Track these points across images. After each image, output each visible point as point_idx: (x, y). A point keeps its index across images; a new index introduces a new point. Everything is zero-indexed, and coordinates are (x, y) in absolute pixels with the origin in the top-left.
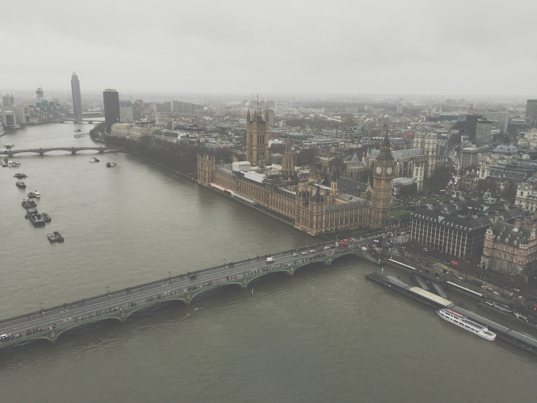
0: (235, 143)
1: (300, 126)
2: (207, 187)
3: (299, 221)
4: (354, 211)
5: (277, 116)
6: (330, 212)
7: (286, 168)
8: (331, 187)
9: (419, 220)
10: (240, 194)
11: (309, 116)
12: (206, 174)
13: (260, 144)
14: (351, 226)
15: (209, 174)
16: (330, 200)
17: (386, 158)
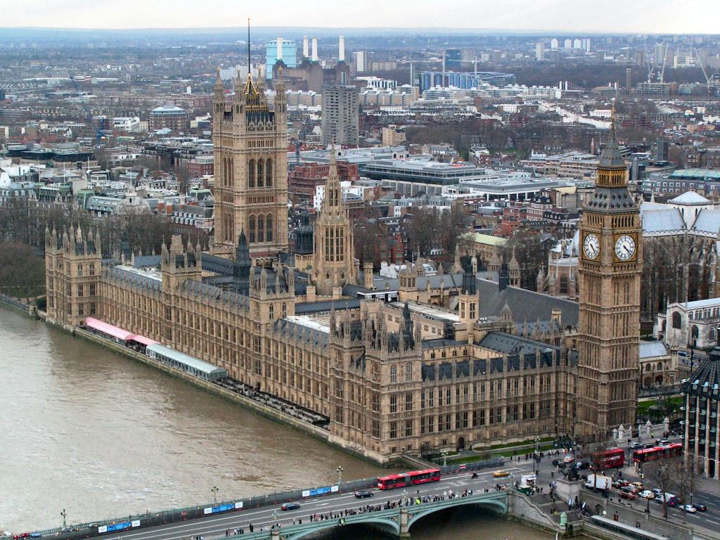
0: (193, 195)
1: (451, 143)
2: (74, 334)
3: (340, 419)
4: (521, 385)
5: (384, 112)
6: (437, 384)
7: (327, 260)
8: (460, 312)
9: (704, 399)
10: (176, 348)
11: (499, 110)
12: (72, 288)
13: (256, 188)
14: (512, 433)
15: (81, 287)
16: (455, 353)
17: (613, 206)
